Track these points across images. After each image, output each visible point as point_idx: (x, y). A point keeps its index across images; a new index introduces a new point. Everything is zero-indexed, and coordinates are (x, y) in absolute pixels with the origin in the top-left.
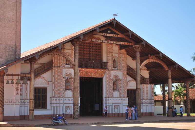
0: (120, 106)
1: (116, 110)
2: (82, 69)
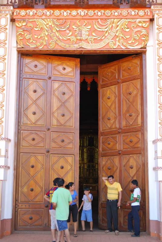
2: (23, 12)
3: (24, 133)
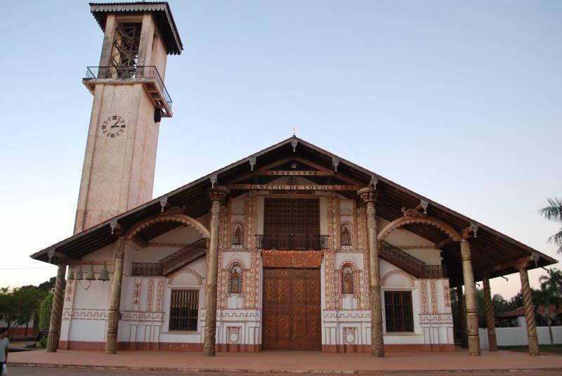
1: (350, 338)
2: (266, 252)
3: (266, 305)
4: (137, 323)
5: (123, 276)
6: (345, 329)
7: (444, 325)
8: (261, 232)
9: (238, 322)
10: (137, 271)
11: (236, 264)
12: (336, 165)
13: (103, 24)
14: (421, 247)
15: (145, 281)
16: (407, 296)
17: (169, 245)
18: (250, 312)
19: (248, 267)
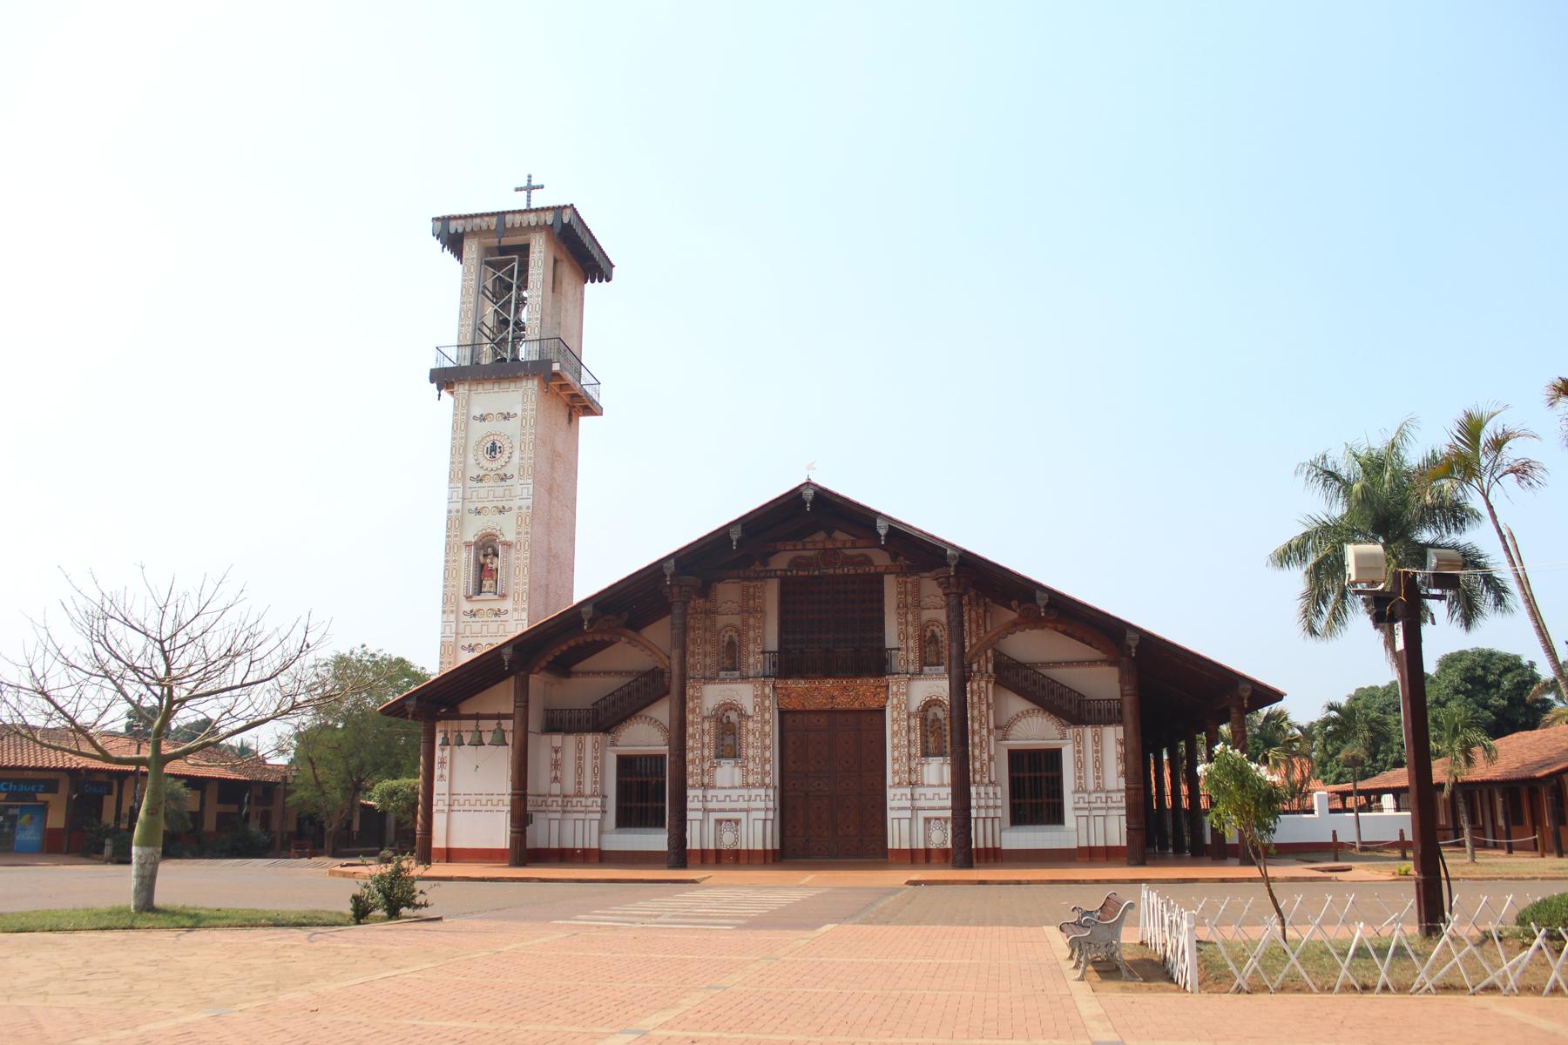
0: (744, 823)
4: (558, 816)
5: (530, 736)
6: (927, 820)
7: (1114, 812)
8: (772, 643)
9: (735, 810)
10: (556, 723)
11: (729, 706)
12: (882, 532)
13: (458, 254)
14: (1080, 663)
15: (571, 740)
16: (1052, 758)
17: (608, 673)
18: (754, 792)
19: (750, 712)
